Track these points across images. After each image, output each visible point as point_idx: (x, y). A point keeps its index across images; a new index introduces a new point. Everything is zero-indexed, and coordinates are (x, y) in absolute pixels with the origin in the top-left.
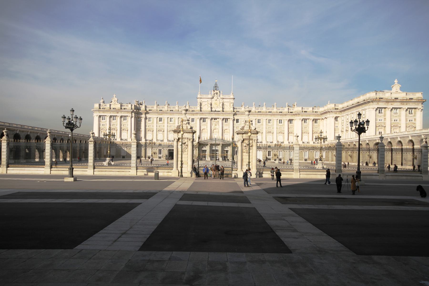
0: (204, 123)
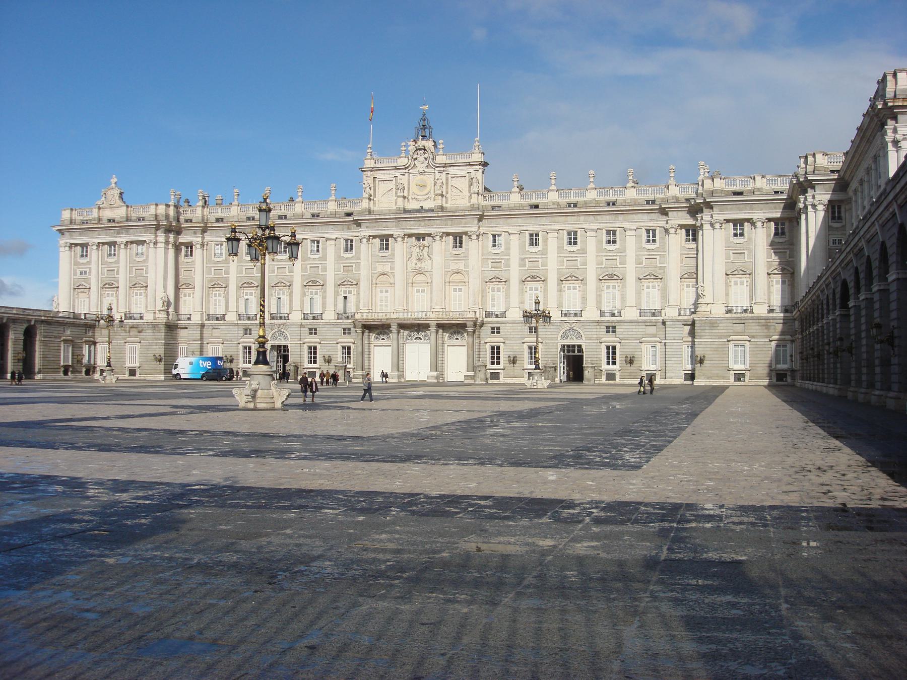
0: (383, 255)
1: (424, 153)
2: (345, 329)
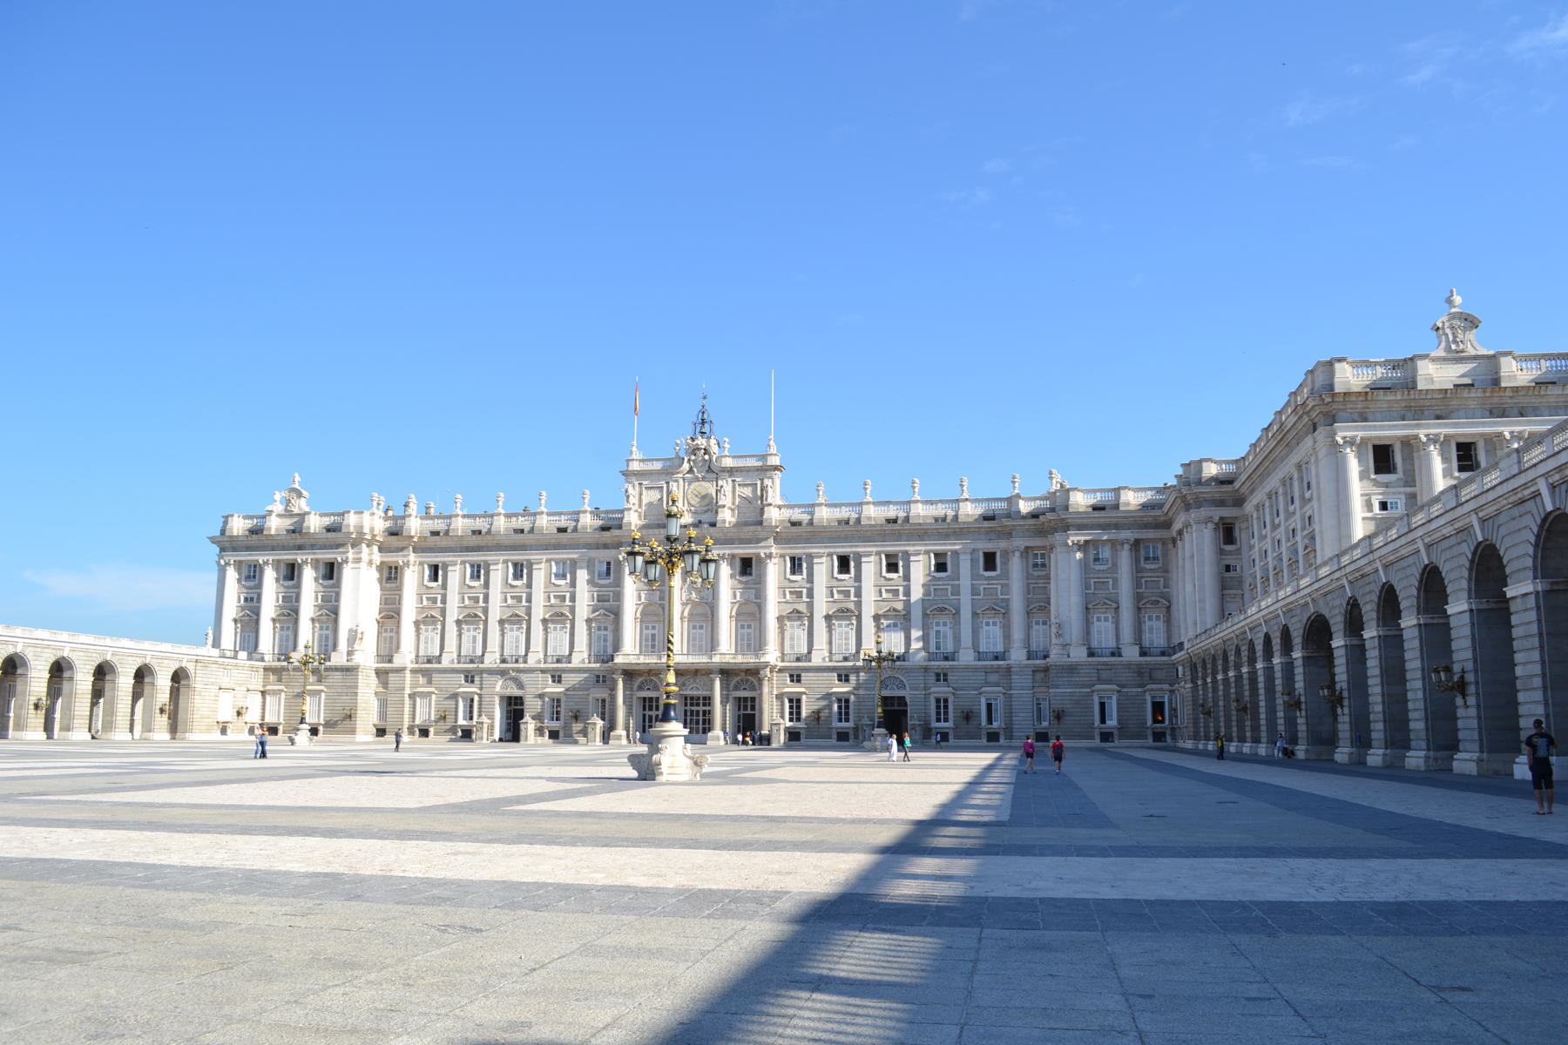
1: (705, 454)
2: (598, 677)
